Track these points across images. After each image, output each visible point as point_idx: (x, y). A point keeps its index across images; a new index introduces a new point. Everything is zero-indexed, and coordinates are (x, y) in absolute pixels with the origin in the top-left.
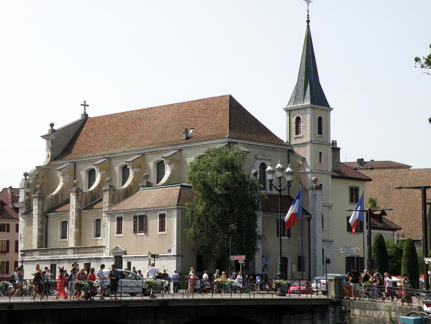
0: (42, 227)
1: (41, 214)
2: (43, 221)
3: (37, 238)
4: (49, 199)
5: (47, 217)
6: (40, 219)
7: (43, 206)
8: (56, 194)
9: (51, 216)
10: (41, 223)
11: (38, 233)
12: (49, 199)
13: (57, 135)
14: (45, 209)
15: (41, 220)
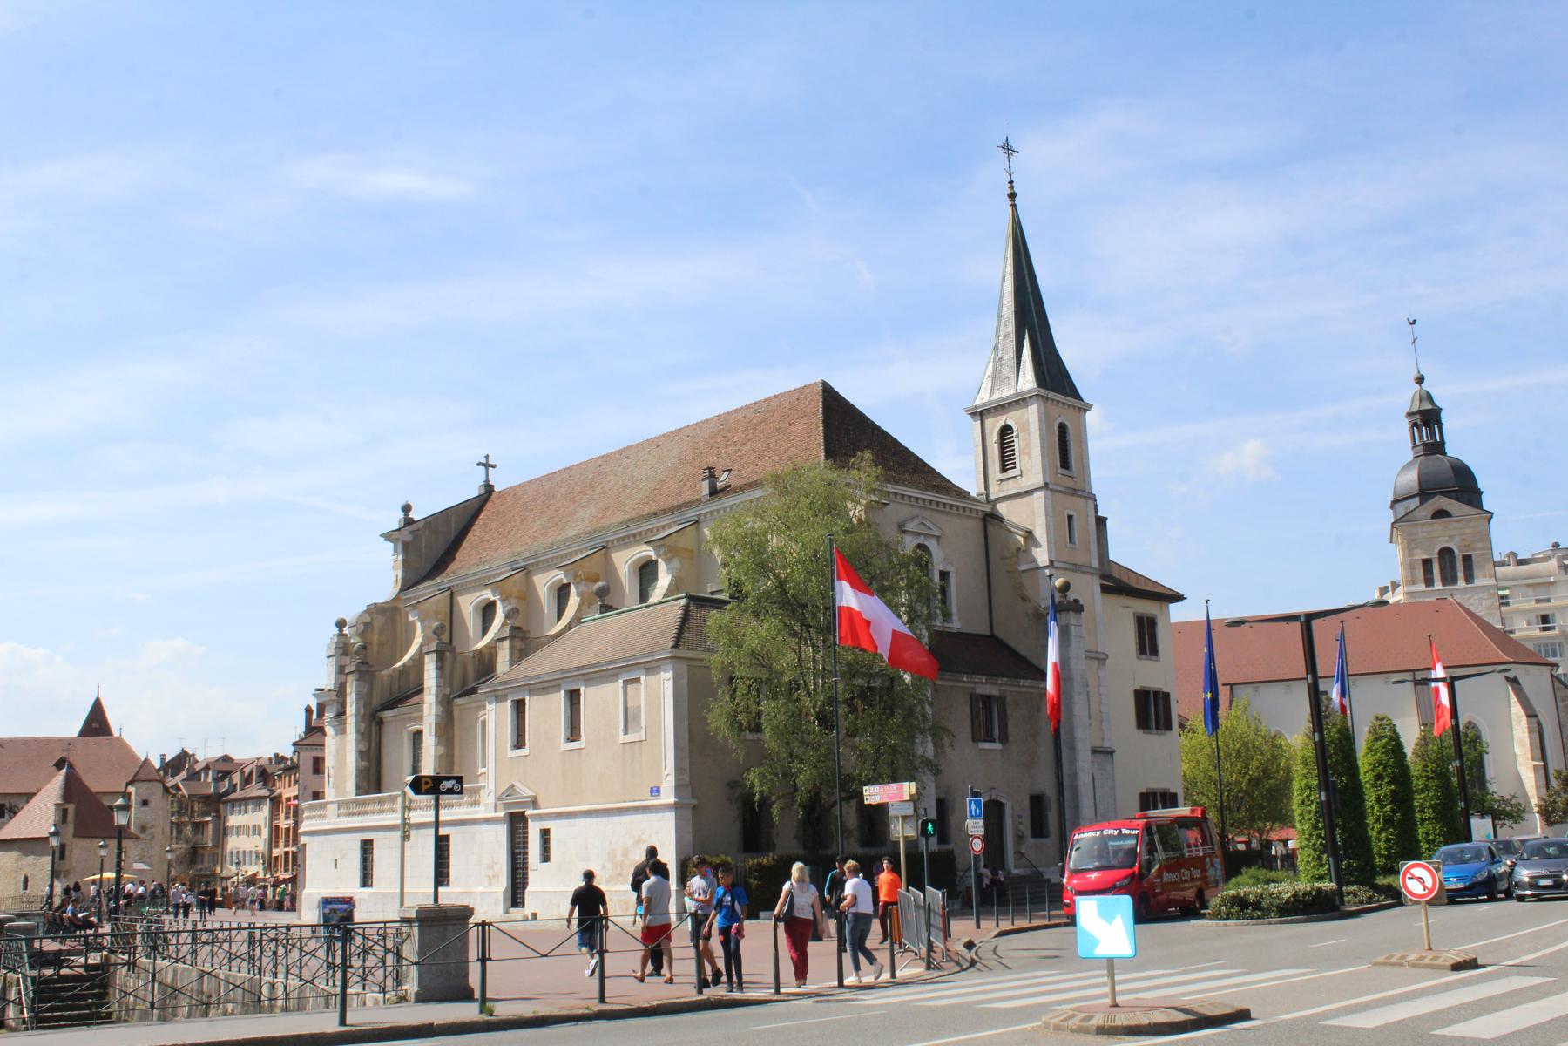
0: (367, 747)
1: (364, 715)
2: (370, 731)
3: (354, 773)
4: (385, 678)
5: (381, 722)
6: (363, 726)
7: (370, 695)
8: (404, 665)
9: (388, 719)
10: (363, 735)
11: (357, 761)
12: (385, 678)
13: (418, 530)
14: (376, 702)
15: (365, 728)
